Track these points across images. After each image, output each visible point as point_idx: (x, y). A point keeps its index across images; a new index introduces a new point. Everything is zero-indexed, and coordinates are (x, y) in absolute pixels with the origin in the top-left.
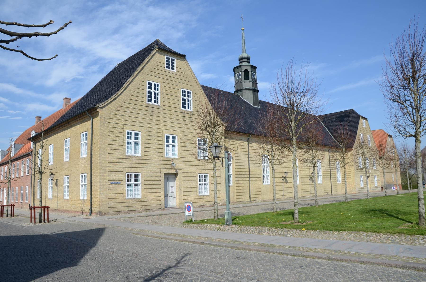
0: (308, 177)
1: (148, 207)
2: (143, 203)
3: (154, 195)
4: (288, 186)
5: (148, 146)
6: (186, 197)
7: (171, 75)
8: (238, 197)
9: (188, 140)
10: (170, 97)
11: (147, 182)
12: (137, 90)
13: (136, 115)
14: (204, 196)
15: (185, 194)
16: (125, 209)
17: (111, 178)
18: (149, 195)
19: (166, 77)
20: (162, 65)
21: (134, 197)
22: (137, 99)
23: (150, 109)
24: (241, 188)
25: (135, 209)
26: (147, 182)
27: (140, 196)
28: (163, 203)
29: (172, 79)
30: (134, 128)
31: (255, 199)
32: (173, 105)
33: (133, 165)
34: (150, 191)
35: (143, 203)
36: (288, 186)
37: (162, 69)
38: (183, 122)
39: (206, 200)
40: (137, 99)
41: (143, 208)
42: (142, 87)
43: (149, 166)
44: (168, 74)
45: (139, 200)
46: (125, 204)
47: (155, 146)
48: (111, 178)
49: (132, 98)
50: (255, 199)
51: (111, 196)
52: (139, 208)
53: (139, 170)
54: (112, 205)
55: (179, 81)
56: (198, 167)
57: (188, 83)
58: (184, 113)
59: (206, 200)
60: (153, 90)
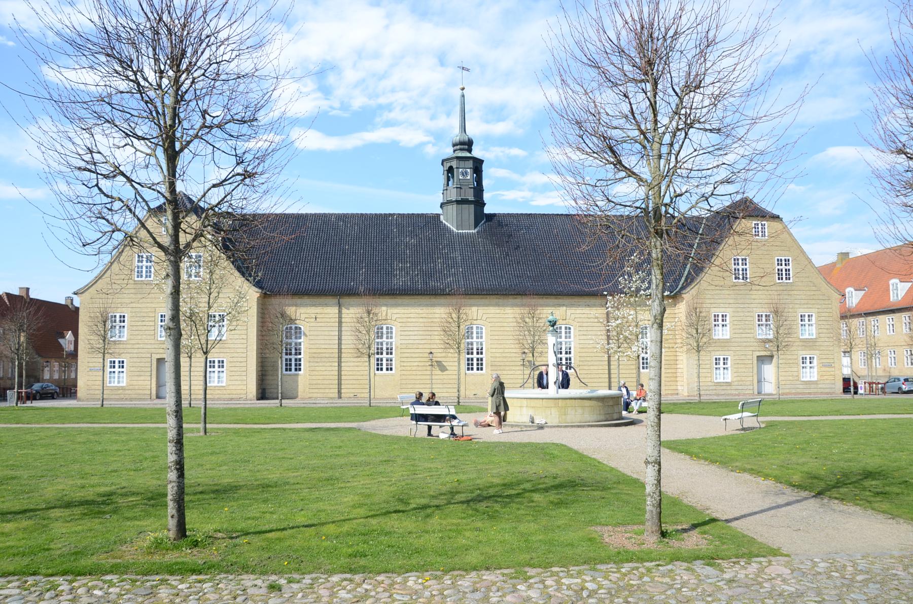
0: (427, 359)
1: (133, 396)
2: (127, 392)
3: (140, 383)
4: (445, 377)
5: (134, 328)
8: (311, 391)
11: (132, 369)
17: (91, 365)
18: (135, 383)
21: (116, 384)
24: (321, 378)
25: (117, 397)
26: (132, 369)
27: (124, 384)
28: (154, 392)
31: (352, 395)
34: (136, 378)
35: (127, 392)
36: (445, 377)
39: (219, 392)
41: (127, 396)
43: (136, 351)
45: (123, 388)
47: (145, 328)
48: (91, 365)
50: (352, 395)
51: (90, 383)
52: (122, 396)
54: (91, 392)
59: (219, 392)
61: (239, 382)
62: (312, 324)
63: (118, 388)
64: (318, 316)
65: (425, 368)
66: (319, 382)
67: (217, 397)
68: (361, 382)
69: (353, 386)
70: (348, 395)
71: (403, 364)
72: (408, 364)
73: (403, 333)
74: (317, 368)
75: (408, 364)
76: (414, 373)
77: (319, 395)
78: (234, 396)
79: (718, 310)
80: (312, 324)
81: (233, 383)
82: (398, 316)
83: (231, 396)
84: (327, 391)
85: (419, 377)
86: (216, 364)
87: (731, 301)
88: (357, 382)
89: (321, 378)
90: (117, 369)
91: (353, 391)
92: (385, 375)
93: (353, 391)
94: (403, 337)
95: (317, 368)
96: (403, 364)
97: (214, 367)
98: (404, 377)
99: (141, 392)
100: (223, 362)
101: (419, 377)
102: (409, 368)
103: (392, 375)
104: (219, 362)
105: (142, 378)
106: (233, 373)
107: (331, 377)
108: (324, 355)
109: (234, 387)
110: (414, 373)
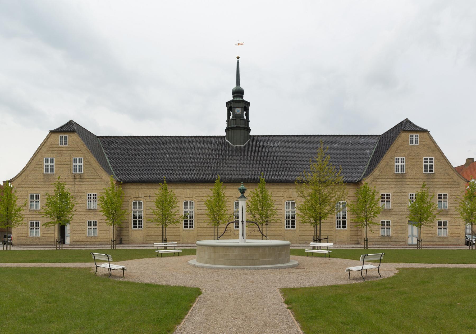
1: (45, 243)
3: (49, 235)
6: (75, 238)
7: (64, 149)
9: (78, 196)
10: (62, 166)
12: (36, 166)
13: (36, 183)
14: (91, 237)
15: (74, 235)
16: (28, 243)
18: (45, 235)
19: (59, 152)
20: (57, 143)
22: (37, 172)
23: (46, 177)
29: (65, 152)
30: (35, 192)
32: (65, 172)
33: (34, 216)
34: (46, 232)
35: (41, 240)
37: (56, 146)
38: (73, 183)
39: (94, 240)
40: (37, 172)
41: (41, 243)
42: (40, 163)
44: (61, 149)
45: (39, 238)
46: (28, 241)
49: (33, 172)
53: (38, 219)
54: (20, 241)
55: (71, 152)
56: (87, 215)
57: (80, 152)
58: (75, 176)
59: (94, 240)
60: (49, 164)
61: (105, 234)
62: (148, 200)
63: (36, 238)
64: (151, 195)
68: (176, 234)
69: (171, 237)
71: (199, 224)
73: (199, 206)
74: (151, 226)
78: (102, 243)
79: (384, 191)
80: (148, 200)
81: (102, 235)
82: (196, 195)
83: (100, 243)
85: (208, 232)
87: (393, 186)
88: (173, 234)
89: (153, 232)
90: (35, 227)
92: (189, 230)
94: (198, 208)
95: (151, 226)
96: (199, 224)
98: (199, 231)
99: (49, 240)
101: (208, 232)
102: (202, 226)
103: (194, 230)
105: (50, 232)
106: (102, 229)
107: (159, 231)
109: (102, 237)
110: (205, 229)
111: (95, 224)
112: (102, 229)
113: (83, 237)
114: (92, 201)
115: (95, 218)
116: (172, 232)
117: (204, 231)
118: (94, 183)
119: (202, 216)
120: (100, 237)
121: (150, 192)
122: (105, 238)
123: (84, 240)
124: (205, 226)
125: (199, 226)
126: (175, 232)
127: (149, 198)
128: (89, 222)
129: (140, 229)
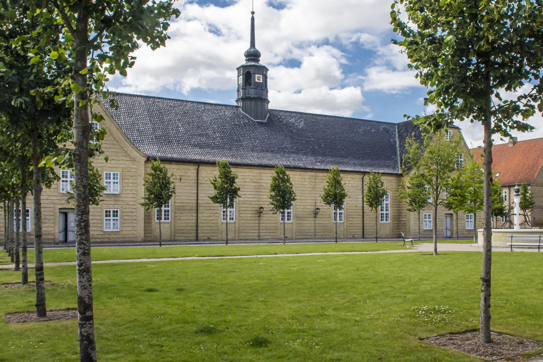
8: (177, 235)
31: (206, 238)
61: (131, 228)
64: (182, 178)
65: (255, 218)
66: (183, 228)
67: (112, 240)
69: (207, 231)
70: (203, 238)
72: (245, 215)
74: (182, 218)
75: (245, 215)
76: (248, 222)
77: (182, 238)
78: (127, 239)
84: (189, 235)
86: (112, 214)
89: (184, 225)
91: (207, 235)
93: (207, 235)
97: (110, 216)
100: (117, 212)
102: (245, 218)
104: (114, 212)
107: (192, 225)
108: (186, 208)
110: (248, 222)
111: (115, 213)
112: (126, 221)
113: (99, 233)
114: (112, 183)
115: (116, 206)
116: (208, 225)
117: (248, 225)
118: (116, 158)
119: (245, 206)
120: (124, 232)
121: (182, 174)
122: (131, 232)
123: (100, 236)
124: (249, 218)
125: (241, 218)
126: (212, 225)
127: (179, 181)
128: (106, 211)
129: (167, 221)
